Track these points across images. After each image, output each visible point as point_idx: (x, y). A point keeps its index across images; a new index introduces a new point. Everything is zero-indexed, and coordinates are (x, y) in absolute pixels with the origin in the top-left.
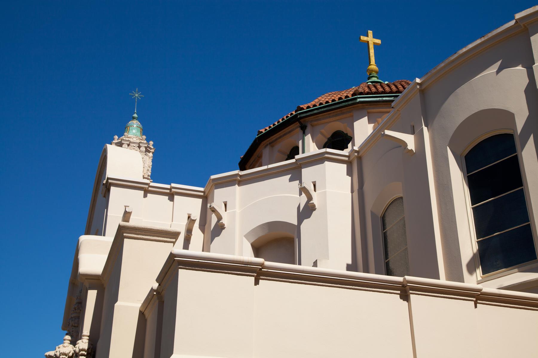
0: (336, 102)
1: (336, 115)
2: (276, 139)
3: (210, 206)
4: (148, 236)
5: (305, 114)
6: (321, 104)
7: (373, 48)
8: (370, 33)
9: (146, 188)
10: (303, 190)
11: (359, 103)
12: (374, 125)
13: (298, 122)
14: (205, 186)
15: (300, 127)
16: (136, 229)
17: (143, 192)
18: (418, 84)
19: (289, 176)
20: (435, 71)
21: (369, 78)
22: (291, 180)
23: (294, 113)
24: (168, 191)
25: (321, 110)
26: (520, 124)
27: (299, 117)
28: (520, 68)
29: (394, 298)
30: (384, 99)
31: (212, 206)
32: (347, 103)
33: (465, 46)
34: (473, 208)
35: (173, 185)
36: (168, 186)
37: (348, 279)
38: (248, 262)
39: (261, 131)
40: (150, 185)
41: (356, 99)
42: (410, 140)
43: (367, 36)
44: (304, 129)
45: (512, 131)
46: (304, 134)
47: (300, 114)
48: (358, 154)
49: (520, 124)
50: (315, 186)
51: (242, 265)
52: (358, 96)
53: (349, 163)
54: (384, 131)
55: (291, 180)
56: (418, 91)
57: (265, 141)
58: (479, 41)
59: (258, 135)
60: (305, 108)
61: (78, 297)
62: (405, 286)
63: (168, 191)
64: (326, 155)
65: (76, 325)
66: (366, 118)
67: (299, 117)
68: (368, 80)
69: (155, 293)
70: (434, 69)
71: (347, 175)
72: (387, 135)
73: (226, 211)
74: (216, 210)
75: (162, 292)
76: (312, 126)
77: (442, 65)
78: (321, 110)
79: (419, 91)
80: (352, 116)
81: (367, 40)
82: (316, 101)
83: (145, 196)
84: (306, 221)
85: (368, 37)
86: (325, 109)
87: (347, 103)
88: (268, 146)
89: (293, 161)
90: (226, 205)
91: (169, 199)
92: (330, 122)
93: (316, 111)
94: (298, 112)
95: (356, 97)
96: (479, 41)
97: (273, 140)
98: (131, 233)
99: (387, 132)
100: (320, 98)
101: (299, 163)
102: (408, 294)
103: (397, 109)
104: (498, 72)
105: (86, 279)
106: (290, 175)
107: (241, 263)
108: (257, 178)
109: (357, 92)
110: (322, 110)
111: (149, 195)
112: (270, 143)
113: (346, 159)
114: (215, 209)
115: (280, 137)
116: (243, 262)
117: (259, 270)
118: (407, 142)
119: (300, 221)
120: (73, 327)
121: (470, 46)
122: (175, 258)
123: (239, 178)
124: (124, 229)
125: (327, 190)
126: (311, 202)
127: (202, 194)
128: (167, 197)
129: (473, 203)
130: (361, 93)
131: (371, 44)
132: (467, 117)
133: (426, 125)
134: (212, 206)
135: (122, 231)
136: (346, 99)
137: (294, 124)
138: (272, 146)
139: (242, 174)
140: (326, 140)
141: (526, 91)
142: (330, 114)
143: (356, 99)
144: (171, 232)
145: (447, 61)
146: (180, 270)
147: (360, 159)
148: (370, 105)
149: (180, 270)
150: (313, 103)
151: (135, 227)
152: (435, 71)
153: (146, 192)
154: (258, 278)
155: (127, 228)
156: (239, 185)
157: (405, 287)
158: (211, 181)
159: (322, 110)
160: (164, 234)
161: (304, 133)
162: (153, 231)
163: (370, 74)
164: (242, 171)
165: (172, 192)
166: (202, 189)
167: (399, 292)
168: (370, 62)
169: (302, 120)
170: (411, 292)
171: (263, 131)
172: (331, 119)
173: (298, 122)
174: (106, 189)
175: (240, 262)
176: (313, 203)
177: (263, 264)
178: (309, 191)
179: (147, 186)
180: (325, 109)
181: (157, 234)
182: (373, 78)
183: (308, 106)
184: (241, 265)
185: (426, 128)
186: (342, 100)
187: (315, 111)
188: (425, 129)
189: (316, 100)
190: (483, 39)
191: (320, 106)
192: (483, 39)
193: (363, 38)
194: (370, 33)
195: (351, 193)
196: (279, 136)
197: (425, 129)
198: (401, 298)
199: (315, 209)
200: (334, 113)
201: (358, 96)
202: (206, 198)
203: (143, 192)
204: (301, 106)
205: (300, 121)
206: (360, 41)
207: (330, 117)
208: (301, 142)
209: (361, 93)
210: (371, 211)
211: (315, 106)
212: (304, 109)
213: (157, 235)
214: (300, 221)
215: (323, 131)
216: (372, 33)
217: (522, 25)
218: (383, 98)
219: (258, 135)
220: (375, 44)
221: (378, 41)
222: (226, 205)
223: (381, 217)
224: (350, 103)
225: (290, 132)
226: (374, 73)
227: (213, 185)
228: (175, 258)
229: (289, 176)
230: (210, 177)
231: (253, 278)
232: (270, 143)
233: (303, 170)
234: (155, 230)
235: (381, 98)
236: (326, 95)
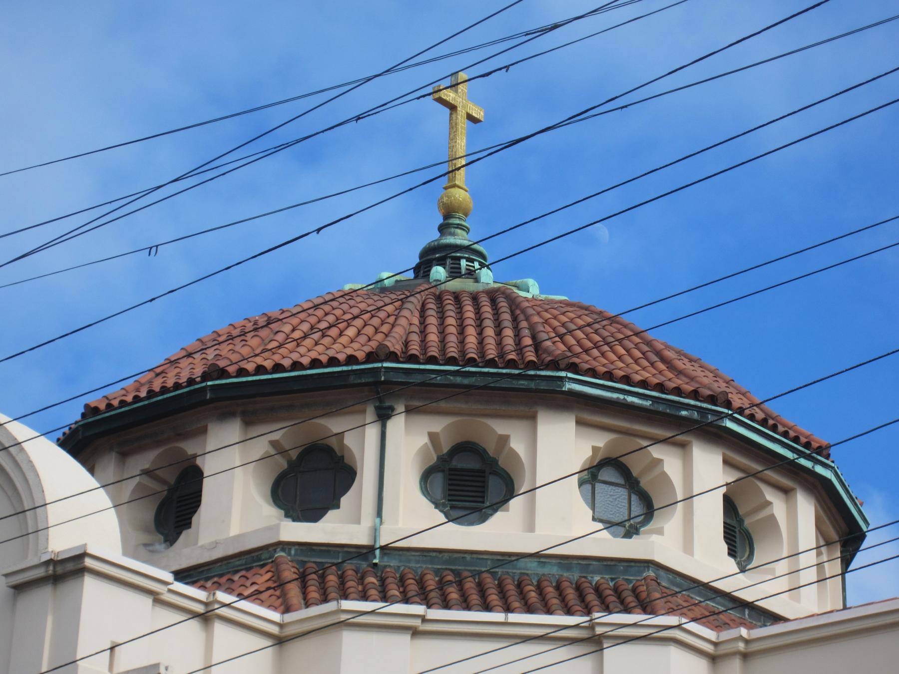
30: (630, 399)
36: (201, 595)
67: (383, 379)
94: (386, 365)
95: (563, 374)
131: (462, 115)
218: (626, 397)
235: (621, 397)
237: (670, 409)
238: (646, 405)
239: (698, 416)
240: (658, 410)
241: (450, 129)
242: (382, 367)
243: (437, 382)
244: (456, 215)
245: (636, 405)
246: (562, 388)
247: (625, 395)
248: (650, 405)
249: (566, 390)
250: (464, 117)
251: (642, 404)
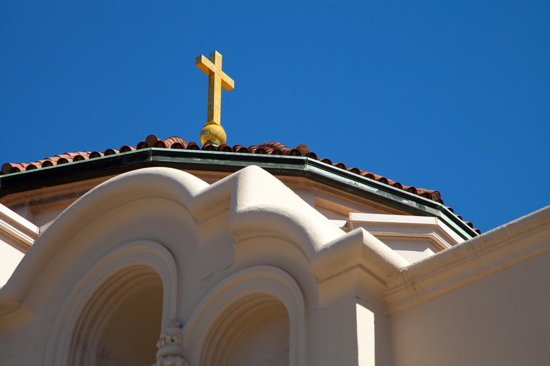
2: (56, 198)
5: (169, 158)
8: (218, 56)
11: (307, 174)
25: (210, 161)
30: (360, 185)
39: (14, 165)
41: (302, 162)
61: (175, 338)
64: (435, 236)
67: (151, 159)
78: (210, 161)
81: (211, 69)
85: (214, 62)
86: (222, 162)
93: (198, 160)
94: (153, 149)
95: (305, 158)
97: (44, 196)
109: (305, 149)
110: (216, 162)
112: (31, 203)
143: (302, 162)
148: (324, 189)
159: (216, 162)
180: (222, 162)
187: (195, 159)
193: (205, 60)
194: (218, 56)
196: (69, 191)
201: (309, 159)
212: (164, 146)
216: (221, 58)
218: (357, 183)
221: (231, 82)
232: (31, 203)
237: (393, 197)
238: (374, 191)
239: (417, 205)
240: (384, 196)
241: (209, 88)
242: (151, 150)
243: (198, 163)
244: (214, 142)
245: (365, 190)
246: (304, 169)
247: (356, 181)
248: (377, 191)
249: (307, 170)
250: (220, 70)
251: (370, 190)
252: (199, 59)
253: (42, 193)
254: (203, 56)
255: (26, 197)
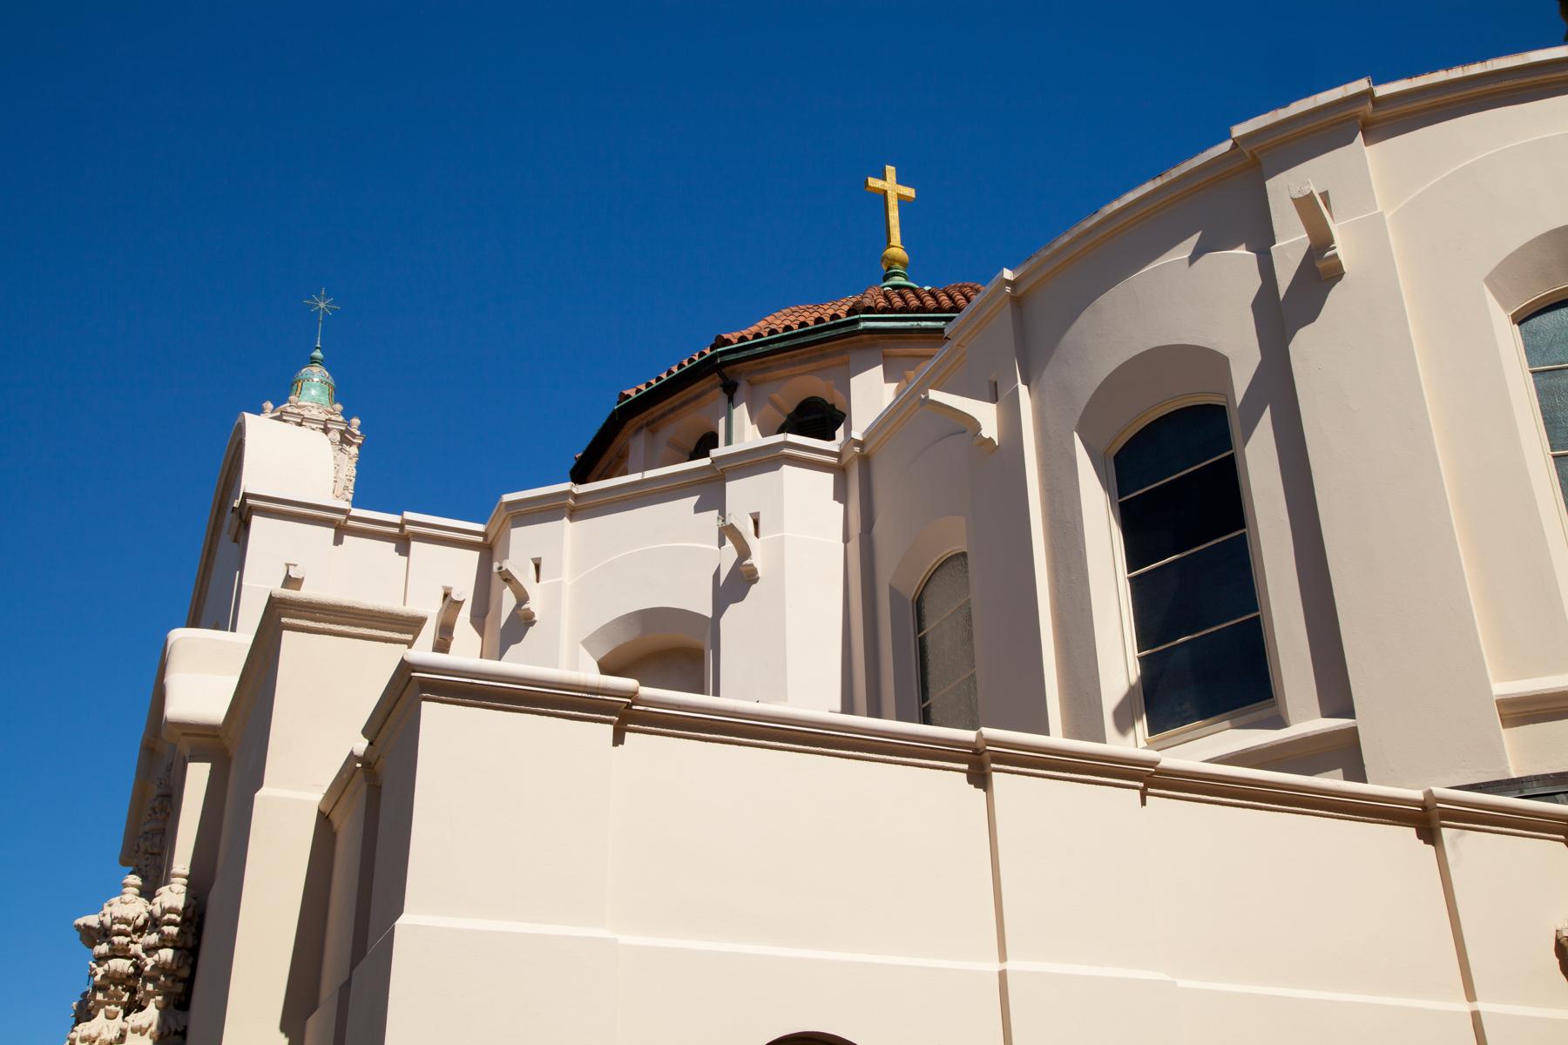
0: (810, 328)
1: (809, 361)
2: (664, 415)
3: (500, 568)
4: (343, 624)
6: (773, 332)
7: (896, 208)
8: (891, 171)
9: (340, 521)
10: (728, 532)
12: (898, 387)
13: (716, 374)
14: (488, 519)
15: (721, 386)
16: (314, 608)
17: (332, 531)
18: (1008, 282)
19: (695, 499)
20: (1048, 252)
21: (886, 278)
22: (699, 508)
23: (708, 352)
24: (396, 530)
26: (1241, 381)
27: (719, 361)
28: (1241, 251)
29: (954, 781)
30: (923, 324)
31: (504, 569)
32: (834, 332)
33: (1117, 195)
34: (1131, 580)
35: (409, 515)
36: (396, 519)
37: (844, 734)
38: (598, 688)
39: (626, 392)
40: (351, 514)
41: (856, 322)
42: (986, 416)
43: (884, 178)
44: (731, 391)
45: (1222, 400)
46: (732, 402)
47: (722, 353)
48: (862, 450)
49: (1241, 381)
50: (756, 523)
51: (584, 695)
52: (862, 316)
53: (840, 472)
54: (926, 393)
55: (699, 508)
56: (1008, 298)
57: (636, 419)
58: (1149, 187)
59: (619, 403)
60: (735, 341)
61: (163, 781)
62: (981, 751)
63: (396, 530)
64: (786, 451)
65: (156, 850)
66: (878, 370)
67: (719, 361)
68: (885, 281)
69: (359, 765)
70: (1046, 248)
71: (835, 499)
72: (933, 401)
73: (538, 581)
74: (514, 578)
75: (378, 763)
76: (752, 384)
77: (1066, 239)
79: (1011, 299)
80: (847, 363)
82: (761, 326)
83: (338, 541)
84: (733, 609)
85: (886, 180)
86: (782, 345)
87: (834, 332)
88: (644, 431)
89: (706, 462)
90: (537, 567)
91: (397, 550)
92: (794, 376)
93: (760, 349)
94: (719, 350)
95: (857, 317)
96: (1149, 187)
97: (655, 415)
98: (301, 618)
99: (935, 395)
100: (769, 319)
101: (718, 469)
102: (988, 770)
103: (957, 343)
104: (1193, 258)
105: (184, 734)
106: (698, 497)
107: (581, 689)
108: (615, 502)
110: (776, 345)
111: (346, 538)
112: (648, 424)
113: (834, 460)
114: (511, 574)
115: (673, 410)
116: (585, 687)
117: (626, 708)
118: (979, 420)
119: (719, 608)
120: (147, 856)
121: (1130, 197)
122: (413, 674)
123: (571, 501)
124: (282, 606)
125: (785, 534)
126: (748, 562)
127: (480, 539)
128: (394, 545)
129: (1131, 566)
130: (869, 310)
132: (1121, 362)
133: (1026, 382)
134: (504, 569)
135: (277, 610)
136: (832, 322)
137: (706, 379)
138: (654, 432)
139: (580, 492)
140: (783, 419)
141: (1257, 306)
142: (795, 356)
143: (856, 322)
144: (402, 616)
145: (1076, 231)
146: (424, 703)
147: (865, 461)
148: (890, 338)
149: (424, 703)
150: (754, 329)
151: (311, 603)
152: (1048, 252)
153: (341, 532)
154: (624, 727)
155: (291, 605)
156: (571, 519)
157: (981, 754)
158: (503, 507)
159: (776, 345)
160: (384, 622)
161: (731, 400)
162: (358, 612)
163: (889, 269)
164: (580, 484)
165: (406, 533)
166: (480, 527)
167: (965, 767)
168: (889, 240)
169: (726, 370)
170: (994, 766)
171: (632, 393)
172: (797, 369)
173: (719, 374)
174: (238, 521)
175: (579, 686)
176: (752, 565)
177: (636, 693)
178: (744, 534)
179: (342, 517)
180: (782, 345)
181: (368, 620)
182: (896, 277)
183: (741, 335)
184: (580, 694)
185: (1026, 387)
186: (824, 324)
188: (1023, 390)
189: (762, 324)
190: (1159, 182)
191: (770, 338)
192: (1159, 182)
193: (874, 182)
194: (891, 171)
195: (844, 542)
197: (1023, 390)
198: (970, 781)
199: (756, 580)
200: (802, 354)
201: (862, 316)
202: (488, 550)
203: (332, 531)
204: (726, 336)
205: (723, 371)
206: (868, 189)
207: (794, 364)
208: (722, 422)
209: (869, 310)
210: (890, 586)
211: (758, 335)
212: (732, 343)
213: (366, 622)
214: (719, 608)
215: (776, 396)
217: (1246, 152)
219: (619, 403)
220: (902, 198)
221: (910, 192)
222: (537, 567)
223: (913, 601)
224: (842, 330)
225: (697, 397)
226: (897, 265)
227: (508, 520)
228: (413, 674)
229: (695, 499)
230: (499, 497)
231: (610, 728)
232: (648, 424)
233: (727, 484)
234: (362, 610)
235: (915, 323)
236: (784, 311)
252: (867, 182)
253: (653, 413)
254: (869, 179)
255: (642, 419)
